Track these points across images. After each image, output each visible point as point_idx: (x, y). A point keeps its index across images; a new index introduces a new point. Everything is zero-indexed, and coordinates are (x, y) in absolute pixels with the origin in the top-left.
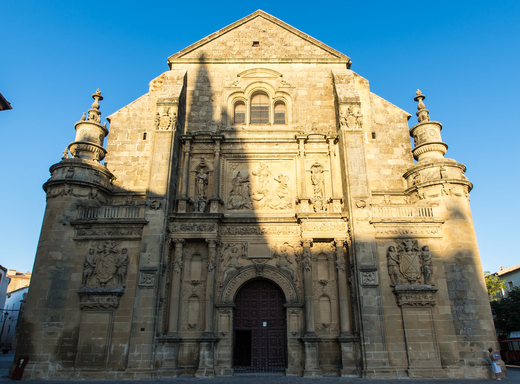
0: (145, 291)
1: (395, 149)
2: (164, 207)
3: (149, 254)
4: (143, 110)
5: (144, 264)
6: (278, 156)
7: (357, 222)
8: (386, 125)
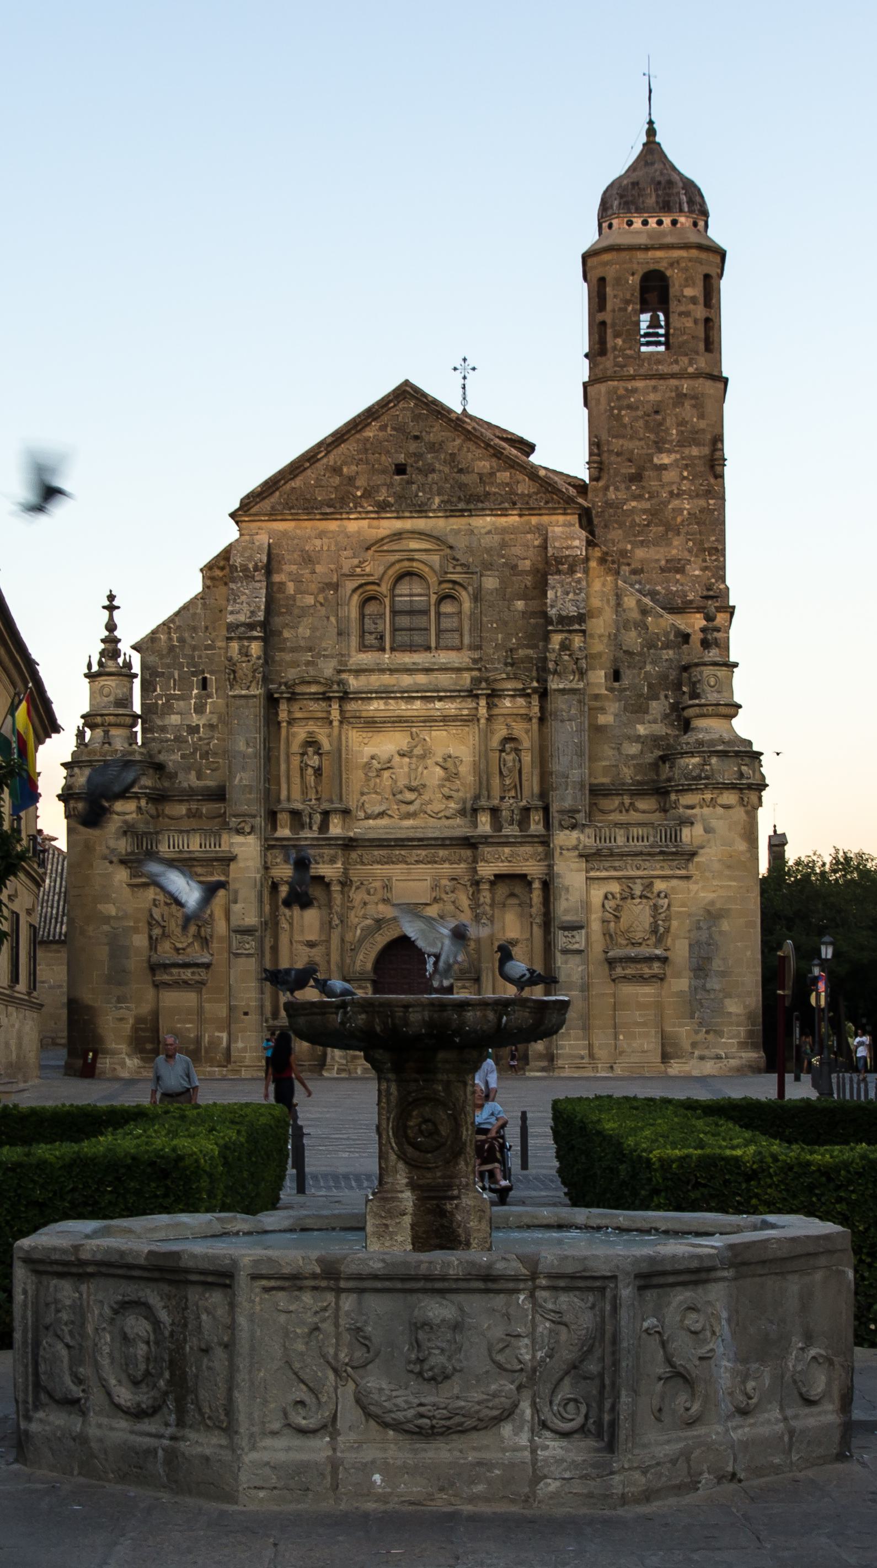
0: (242, 960)
1: (654, 704)
2: (258, 832)
3: (243, 905)
4: (194, 629)
5: (235, 922)
7: (561, 853)
8: (641, 654)
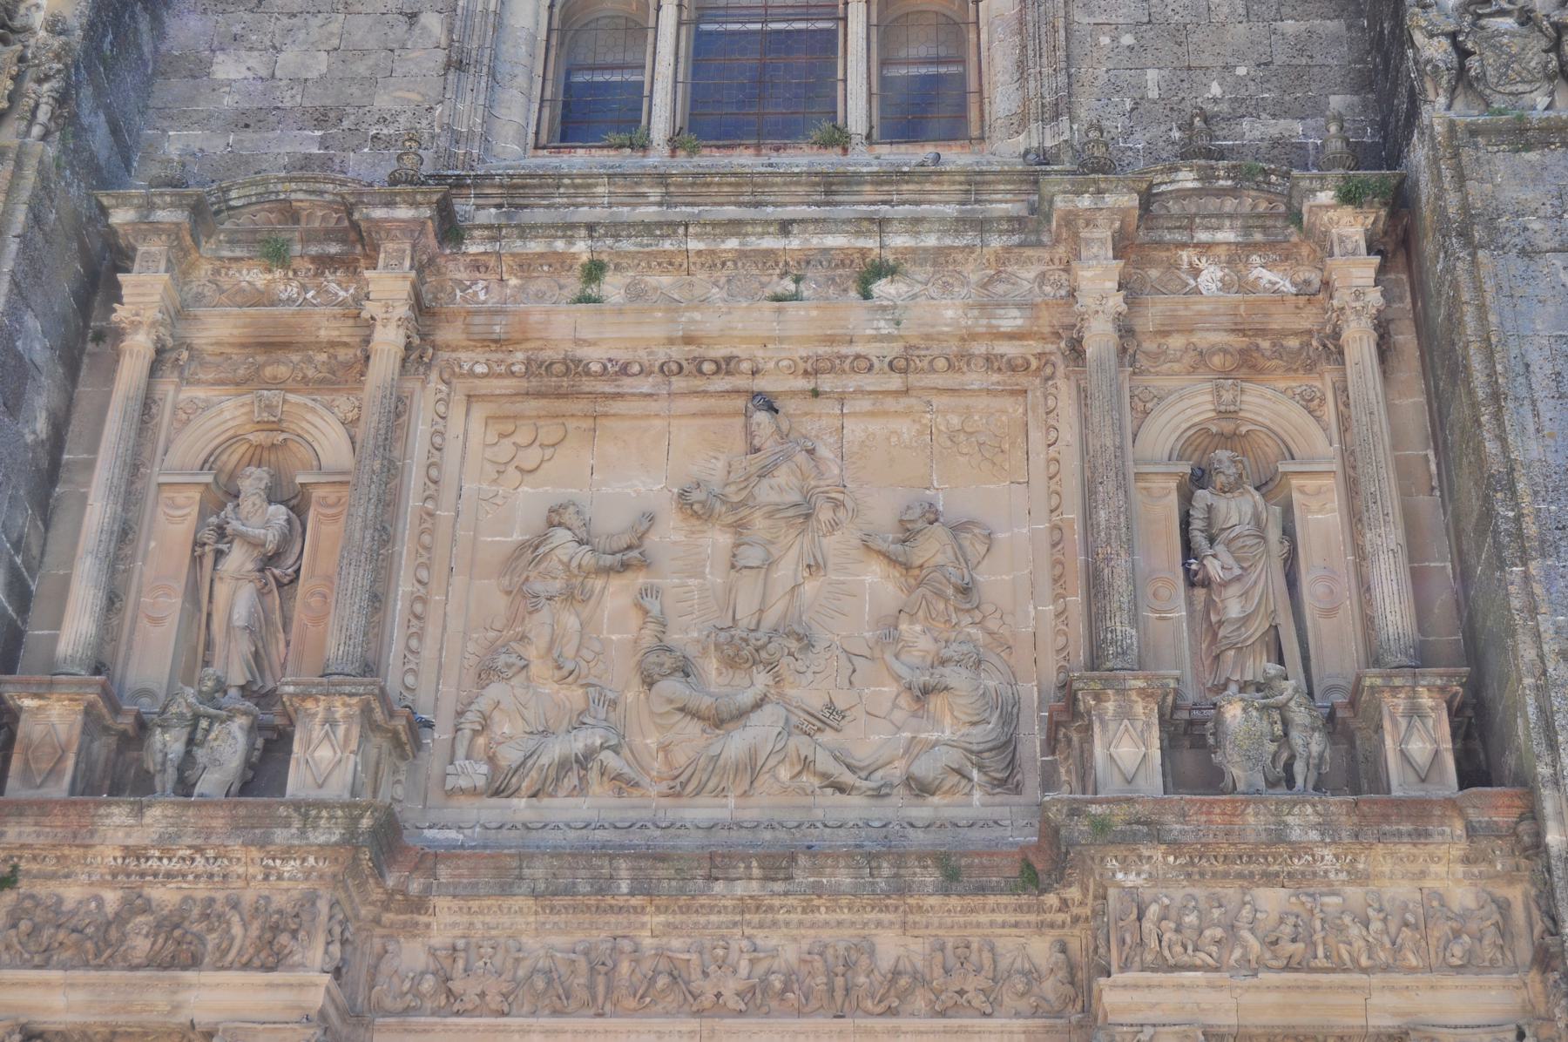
6: (902, 363)
